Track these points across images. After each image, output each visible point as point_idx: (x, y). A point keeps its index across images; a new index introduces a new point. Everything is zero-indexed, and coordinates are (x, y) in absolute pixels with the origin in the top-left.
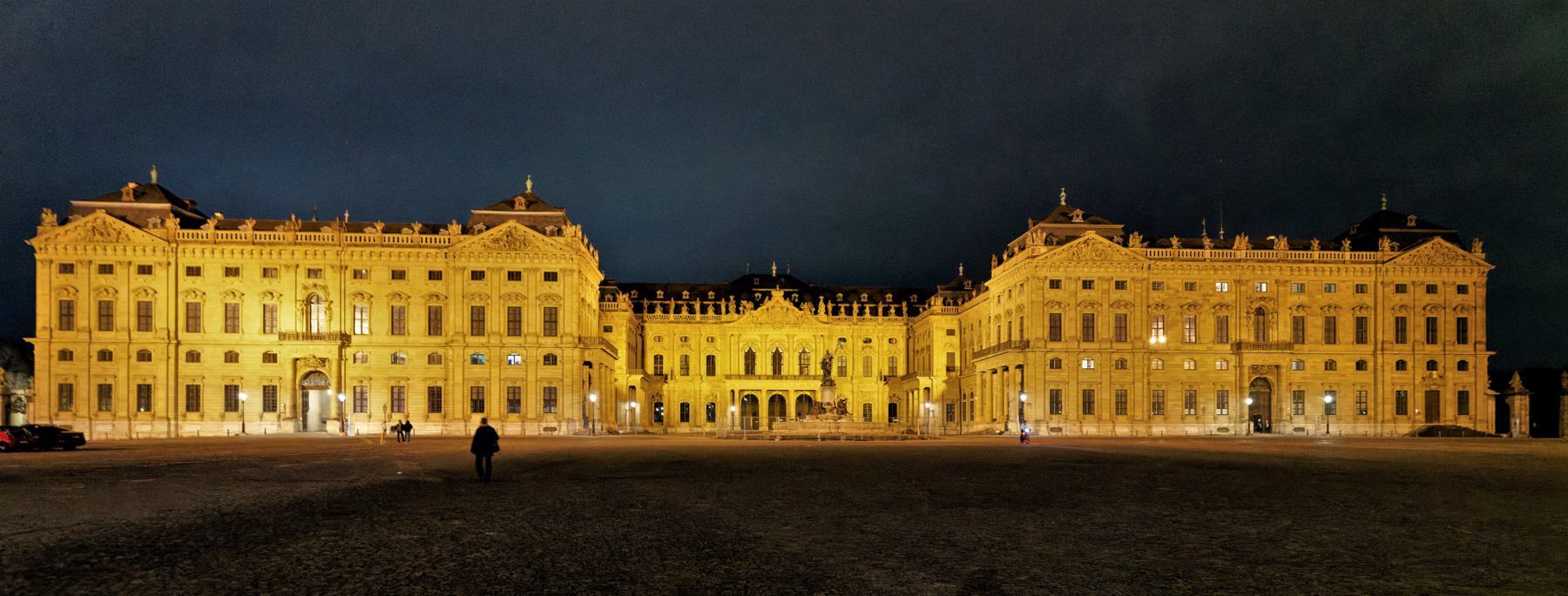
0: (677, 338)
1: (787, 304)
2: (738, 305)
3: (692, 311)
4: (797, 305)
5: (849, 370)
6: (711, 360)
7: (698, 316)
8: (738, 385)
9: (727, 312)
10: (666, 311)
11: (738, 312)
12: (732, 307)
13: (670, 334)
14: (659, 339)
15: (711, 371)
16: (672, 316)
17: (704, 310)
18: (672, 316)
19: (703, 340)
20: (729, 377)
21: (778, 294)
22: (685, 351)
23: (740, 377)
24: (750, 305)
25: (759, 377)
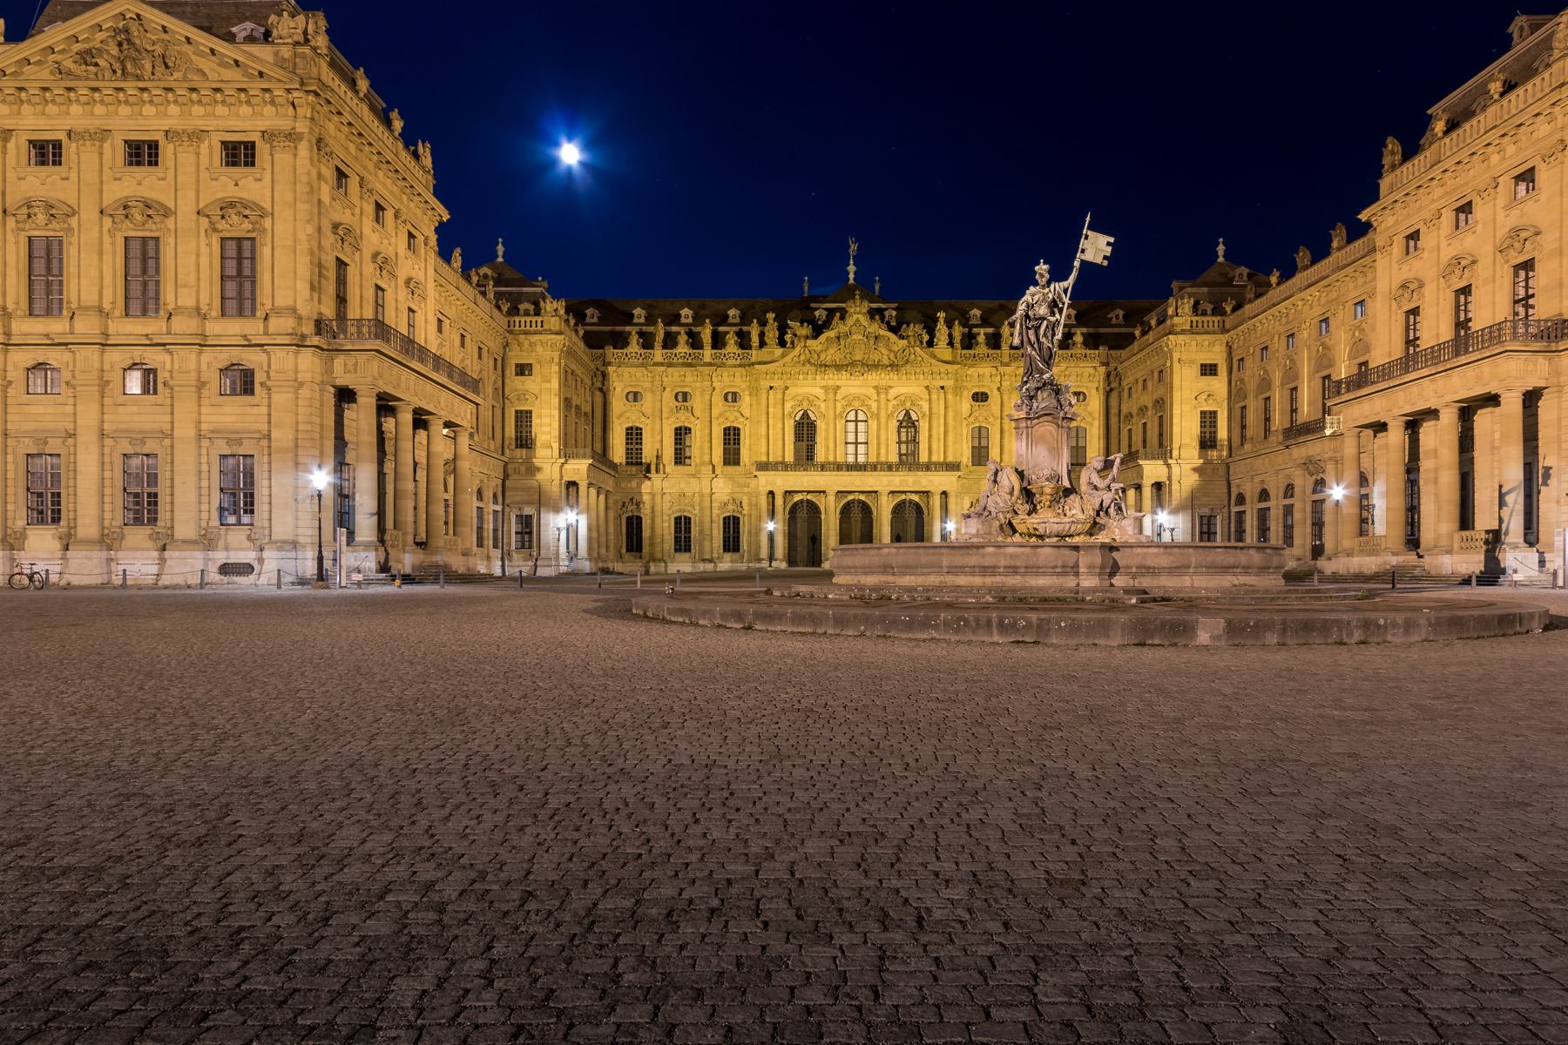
0: (668, 396)
1: (876, 328)
2: (783, 329)
3: (695, 343)
4: (895, 330)
5: (994, 453)
6: (732, 437)
7: (708, 353)
8: (782, 482)
9: (762, 344)
10: (647, 342)
11: (782, 343)
12: (772, 333)
13: (654, 391)
14: (636, 396)
15: (732, 456)
16: (658, 353)
17: (718, 342)
18: (658, 353)
19: (718, 399)
20: (763, 466)
21: (858, 311)
22: (683, 419)
23: (786, 467)
24: (805, 330)
25: (823, 467)
